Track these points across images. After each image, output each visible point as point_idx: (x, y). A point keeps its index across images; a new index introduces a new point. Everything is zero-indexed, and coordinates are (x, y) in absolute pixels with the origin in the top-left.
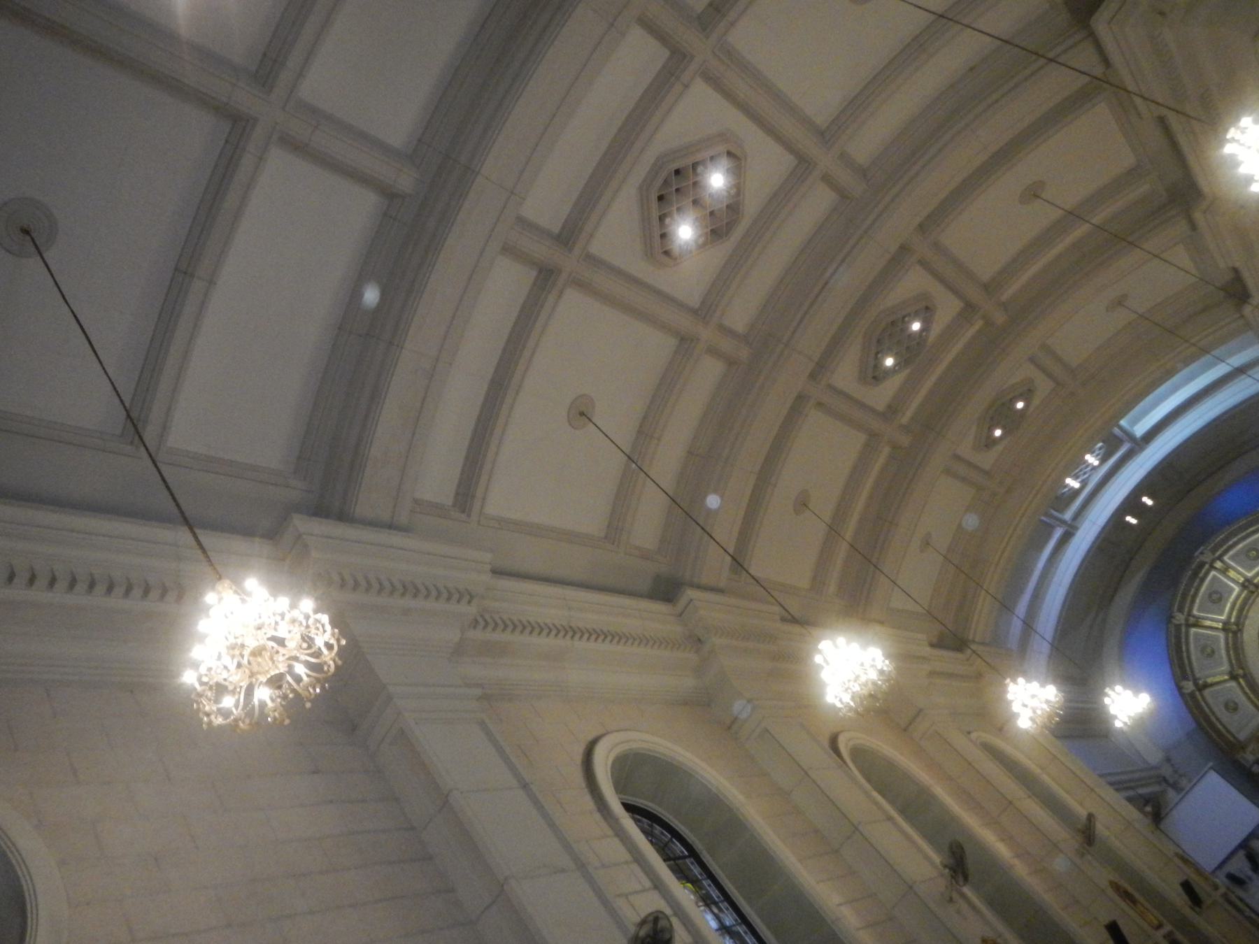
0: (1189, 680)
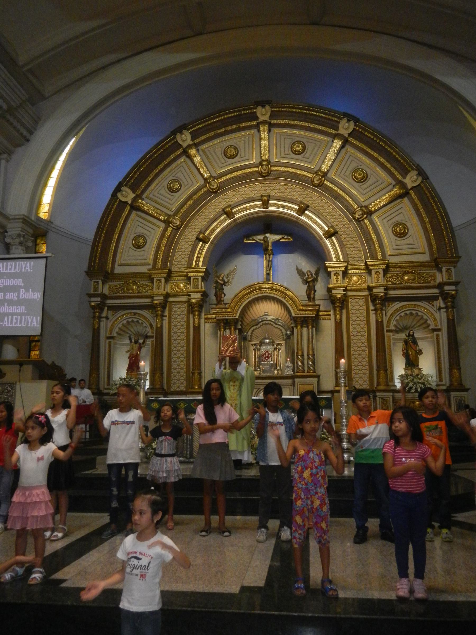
0: (134, 192)
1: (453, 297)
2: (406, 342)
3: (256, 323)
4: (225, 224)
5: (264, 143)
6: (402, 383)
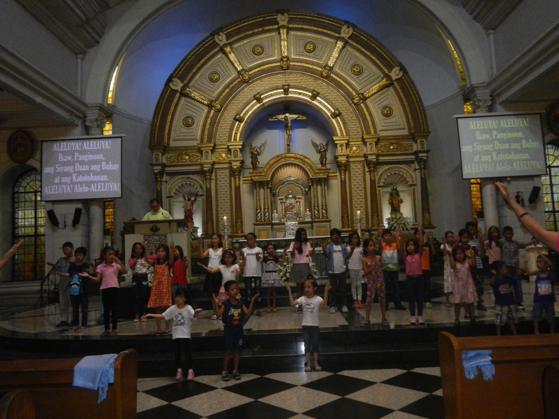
0: (182, 82)
1: (425, 161)
2: (391, 194)
3: (282, 183)
4: (256, 107)
5: (284, 43)
6: (389, 223)
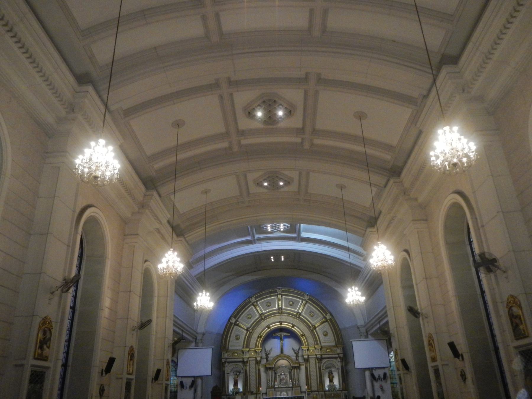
0: (235, 319)
2: (329, 373)
3: (279, 367)
